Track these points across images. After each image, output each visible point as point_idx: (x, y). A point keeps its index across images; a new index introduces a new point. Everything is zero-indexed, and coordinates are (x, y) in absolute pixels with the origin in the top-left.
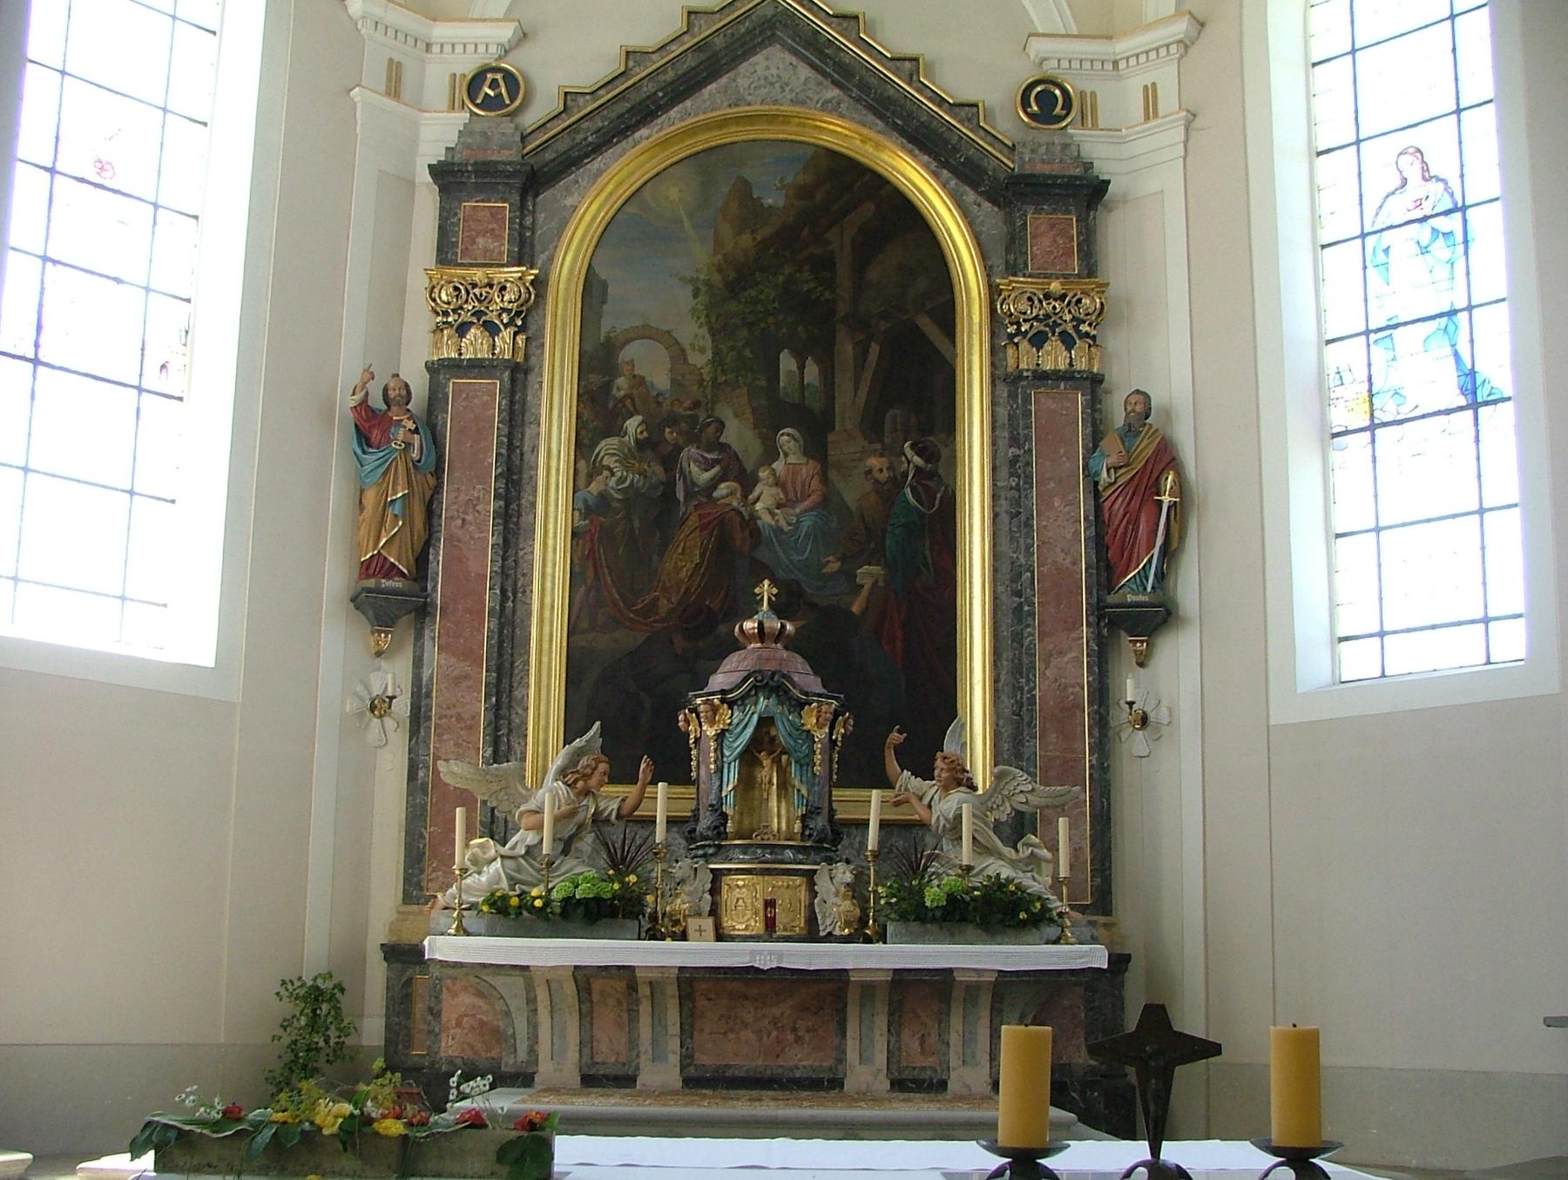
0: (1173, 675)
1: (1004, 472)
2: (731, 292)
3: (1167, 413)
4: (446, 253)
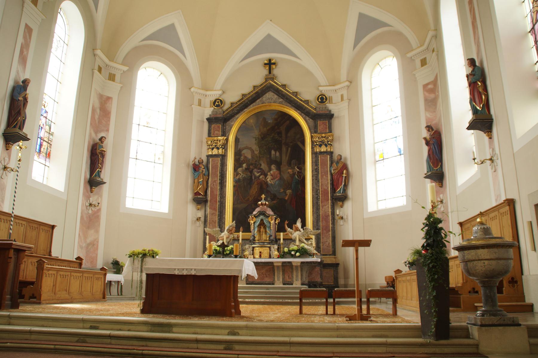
0: (347, 210)
1: (314, 171)
2: (262, 139)
3: (346, 159)
4: (209, 135)
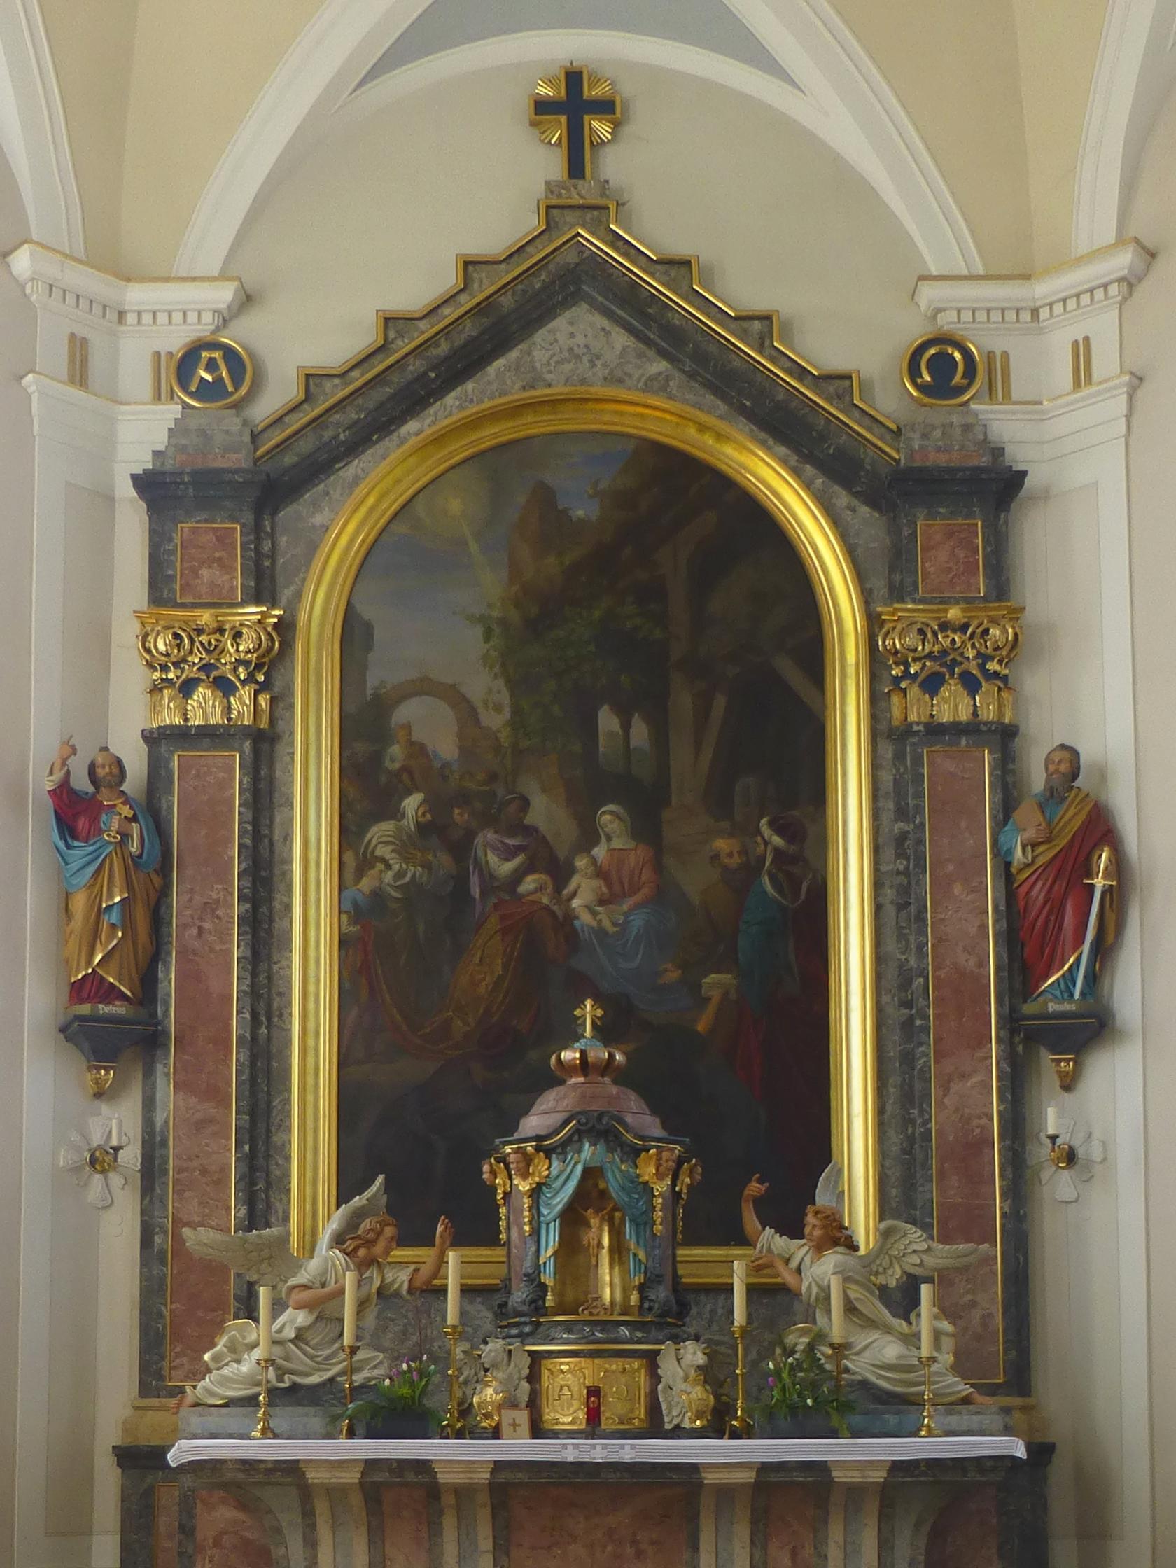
2: (529, 629)
3: (1102, 774)
